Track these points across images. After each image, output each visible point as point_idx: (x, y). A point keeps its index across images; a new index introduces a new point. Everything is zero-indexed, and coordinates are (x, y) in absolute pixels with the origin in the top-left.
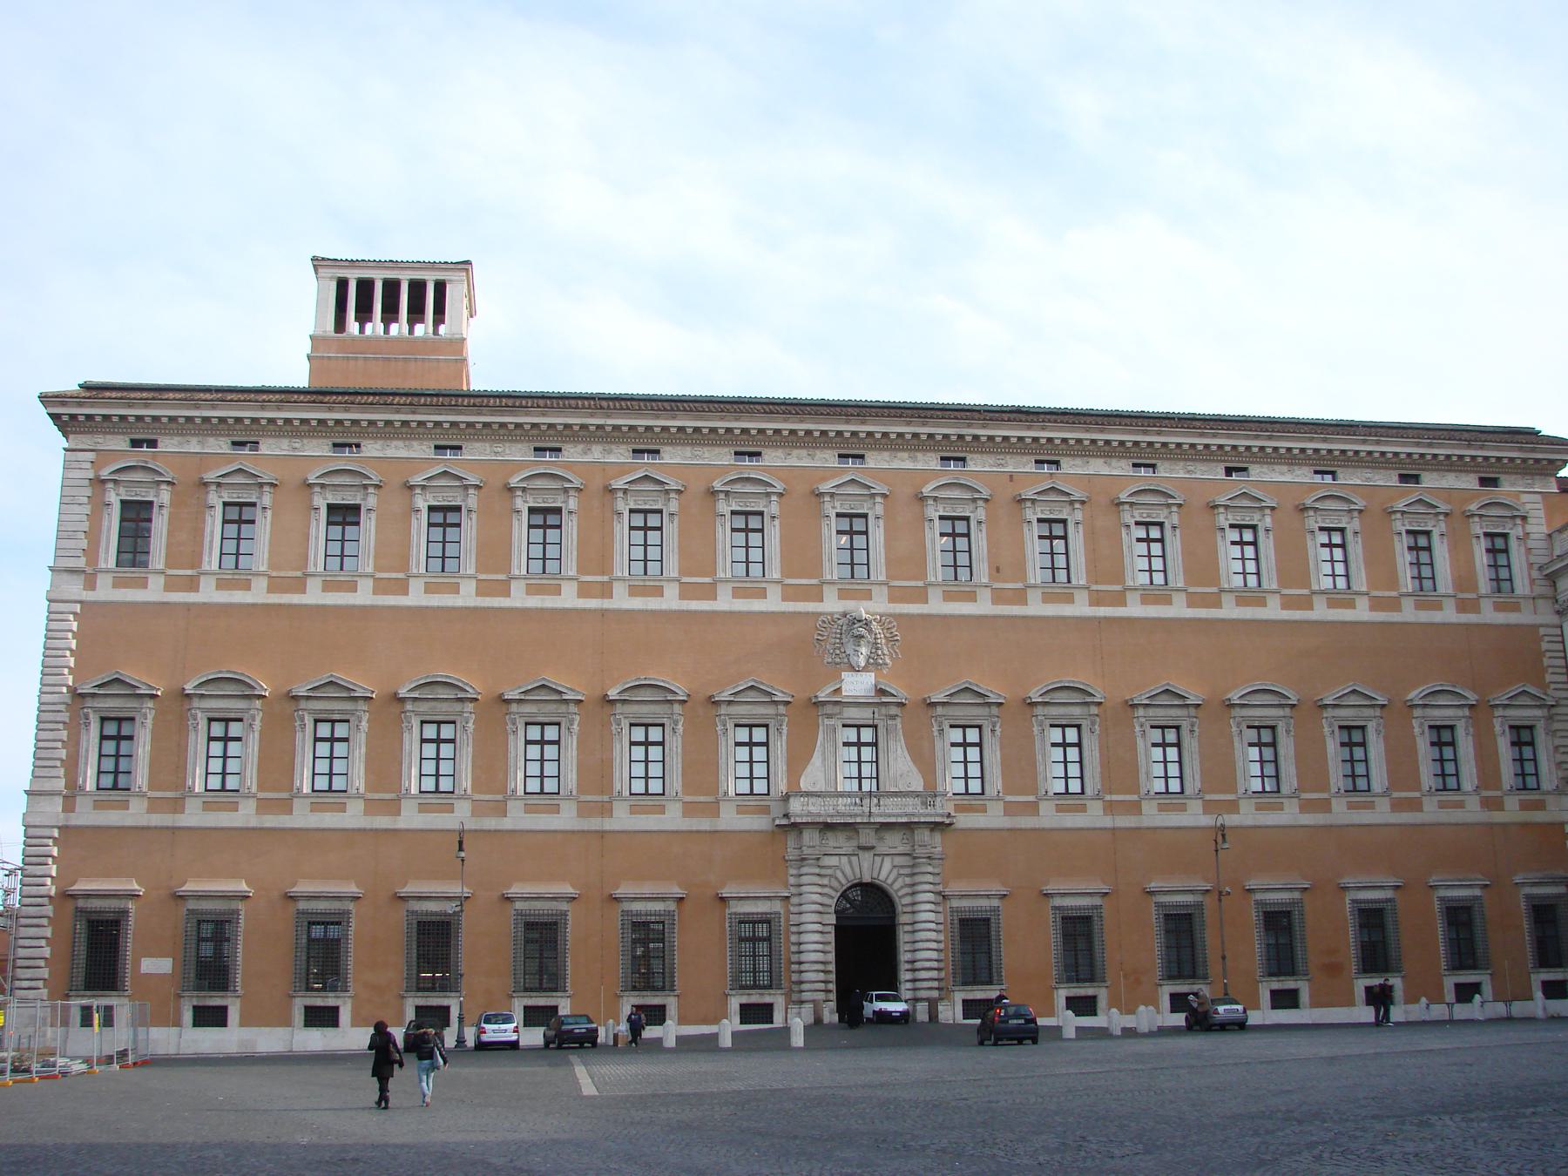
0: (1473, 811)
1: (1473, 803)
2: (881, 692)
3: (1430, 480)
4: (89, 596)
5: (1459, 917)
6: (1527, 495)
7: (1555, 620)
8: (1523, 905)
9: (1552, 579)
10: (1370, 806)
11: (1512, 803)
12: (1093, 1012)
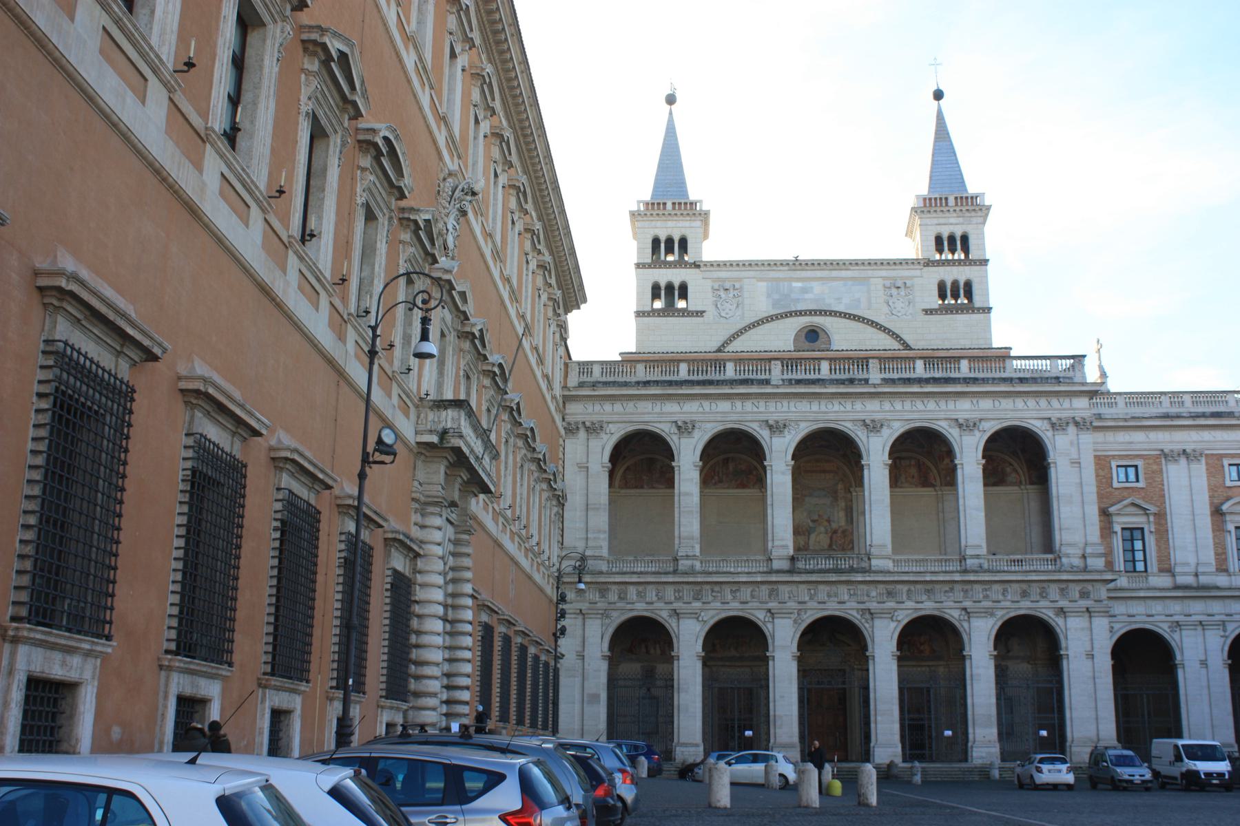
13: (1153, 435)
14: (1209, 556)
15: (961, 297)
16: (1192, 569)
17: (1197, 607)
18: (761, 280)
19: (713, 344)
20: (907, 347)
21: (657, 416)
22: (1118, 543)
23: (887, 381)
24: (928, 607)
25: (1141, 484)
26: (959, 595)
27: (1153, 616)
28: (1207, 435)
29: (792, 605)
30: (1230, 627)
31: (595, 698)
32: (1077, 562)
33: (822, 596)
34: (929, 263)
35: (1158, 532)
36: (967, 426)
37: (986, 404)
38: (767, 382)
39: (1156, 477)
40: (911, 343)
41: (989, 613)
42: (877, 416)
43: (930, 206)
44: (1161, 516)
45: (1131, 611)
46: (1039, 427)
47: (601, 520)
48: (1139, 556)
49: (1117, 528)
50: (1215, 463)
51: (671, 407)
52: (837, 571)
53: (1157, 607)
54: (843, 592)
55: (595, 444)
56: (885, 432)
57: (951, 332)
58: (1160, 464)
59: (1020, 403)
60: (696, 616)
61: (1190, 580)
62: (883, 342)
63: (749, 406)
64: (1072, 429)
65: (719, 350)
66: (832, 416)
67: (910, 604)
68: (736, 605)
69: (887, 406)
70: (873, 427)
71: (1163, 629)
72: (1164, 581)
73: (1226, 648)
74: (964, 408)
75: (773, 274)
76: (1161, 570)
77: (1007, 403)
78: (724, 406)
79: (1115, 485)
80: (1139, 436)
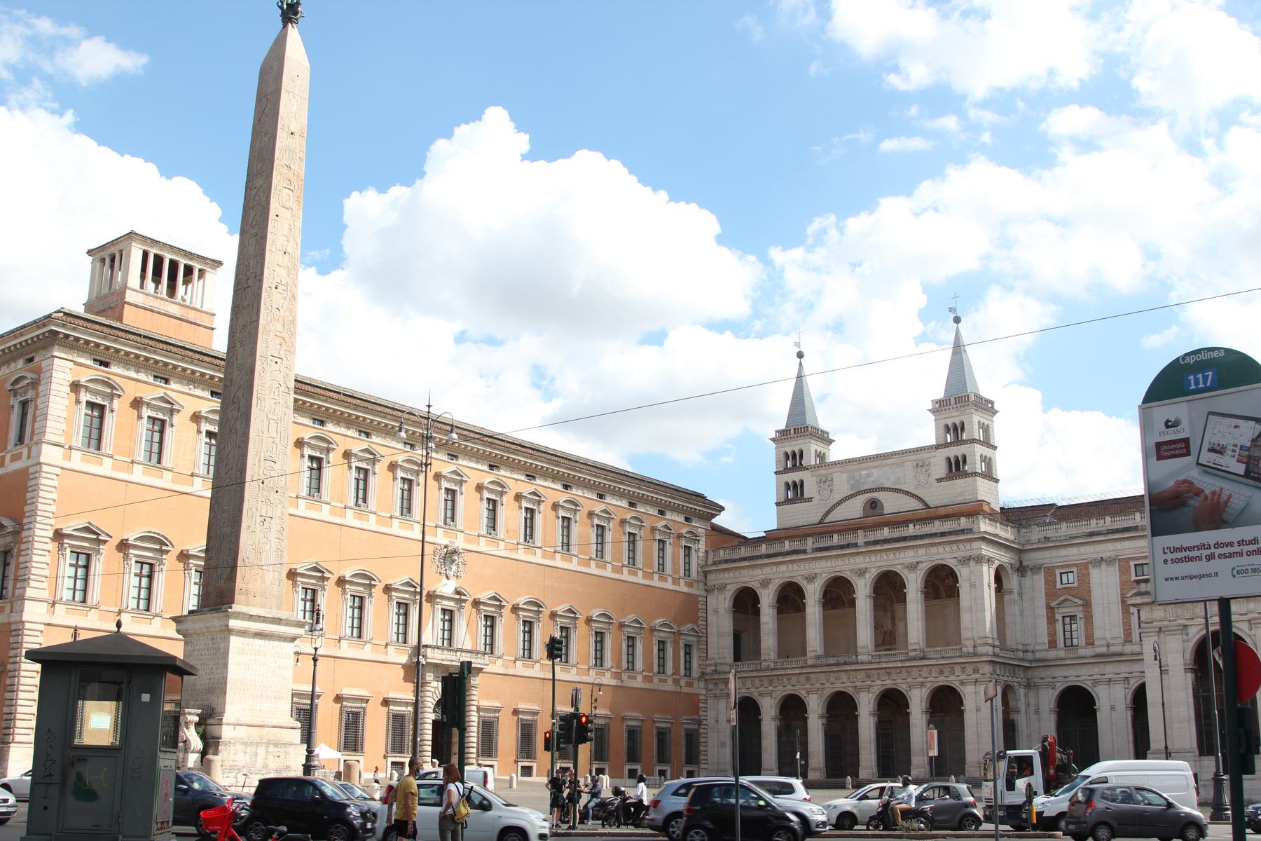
0: (669, 686)
1: (670, 681)
2: (458, 592)
3: (669, 515)
4: (67, 465)
5: (662, 735)
6: (699, 527)
7: (704, 593)
8: (683, 734)
9: (706, 574)
10: (635, 678)
11: (683, 682)
12: (530, 775)
13: (1083, 549)
14: (1119, 632)
15: (957, 468)
16: (1104, 642)
17: (1110, 670)
18: (842, 472)
19: (817, 519)
20: (928, 507)
21: (750, 577)
22: (1059, 626)
23: (867, 544)
24: (889, 684)
25: (1076, 585)
26: (904, 675)
27: (1081, 676)
28: (1118, 545)
29: (818, 685)
30: (1132, 681)
31: (723, 744)
32: (971, 650)
33: (832, 680)
34: (938, 447)
35: (1086, 617)
36: (913, 567)
37: (922, 551)
38: (804, 552)
39: (1084, 578)
40: (930, 504)
41: (922, 685)
42: (863, 566)
43: (940, 407)
44: (1087, 605)
45: (1066, 674)
46: (952, 563)
47: (728, 642)
48: (1068, 635)
49: (1059, 617)
50: (1123, 563)
51: (757, 572)
52: (838, 664)
53: (1083, 671)
54: (844, 677)
55: (721, 597)
56: (868, 575)
57: (955, 491)
58: (1087, 569)
59: (941, 549)
60: (770, 695)
61: (1104, 650)
62: (915, 505)
63: (795, 567)
64: (972, 563)
65: (820, 522)
66: (837, 569)
67: (879, 682)
68: (789, 687)
69: (867, 559)
70: (861, 573)
71: (1088, 685)
72: (1089, 651)
73: (1129, 696)
74: (909, 556)
75: (850, 468)
76: (1088, 644)
77: (933, 550)
78: (783, 568)
79: (1059, 586)
80: (1074, 551)
